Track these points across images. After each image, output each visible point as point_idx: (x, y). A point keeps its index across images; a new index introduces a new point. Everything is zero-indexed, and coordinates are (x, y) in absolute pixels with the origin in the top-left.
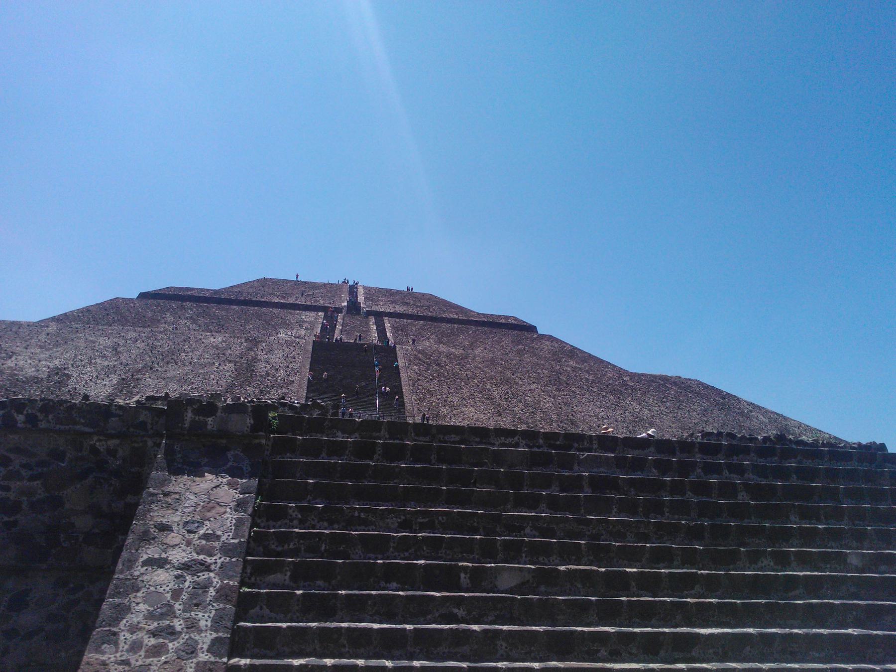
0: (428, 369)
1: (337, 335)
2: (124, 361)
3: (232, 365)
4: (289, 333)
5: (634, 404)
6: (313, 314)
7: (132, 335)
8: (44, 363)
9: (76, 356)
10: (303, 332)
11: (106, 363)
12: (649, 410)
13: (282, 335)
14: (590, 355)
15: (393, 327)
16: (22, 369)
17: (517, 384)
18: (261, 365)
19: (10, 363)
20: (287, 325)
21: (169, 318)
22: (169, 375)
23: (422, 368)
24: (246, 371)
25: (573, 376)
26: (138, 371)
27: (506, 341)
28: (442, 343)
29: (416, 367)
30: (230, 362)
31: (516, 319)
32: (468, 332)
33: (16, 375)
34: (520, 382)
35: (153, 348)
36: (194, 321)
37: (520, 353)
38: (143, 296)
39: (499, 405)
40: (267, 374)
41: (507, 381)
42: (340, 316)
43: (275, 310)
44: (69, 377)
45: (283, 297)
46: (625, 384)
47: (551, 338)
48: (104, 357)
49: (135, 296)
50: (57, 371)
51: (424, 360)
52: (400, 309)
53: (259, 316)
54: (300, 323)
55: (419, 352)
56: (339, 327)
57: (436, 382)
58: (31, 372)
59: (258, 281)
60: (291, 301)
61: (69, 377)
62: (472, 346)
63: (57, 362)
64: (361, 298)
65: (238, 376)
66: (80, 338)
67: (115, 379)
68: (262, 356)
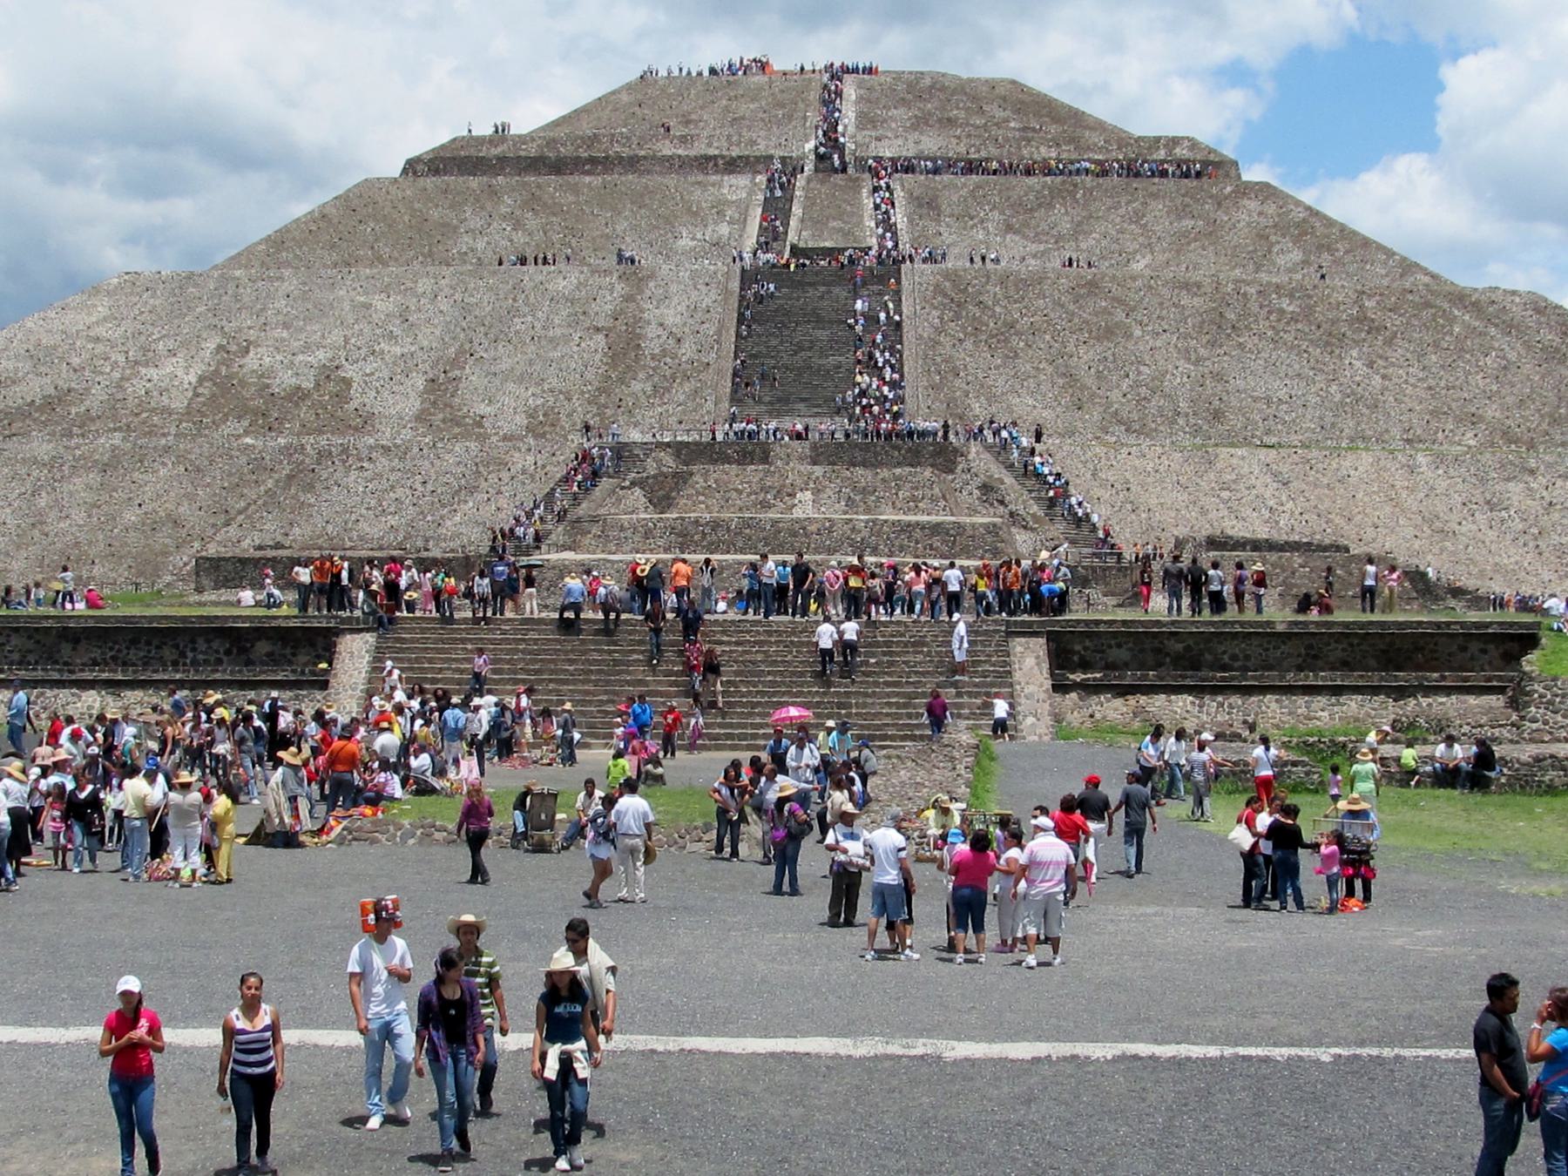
0: (957, 317)
1: (795, 234)
2: (425, 343)
3: (600, 337)
4: (699, 236)
5: (1358, 364)
6: (742, 181)
7: (424, 285)
8: (301, 357)
9: (346, 341)
10: (724, 229)
11: (398, 350)
12: (1384, 377)
13: (685, 243)
14: (1342, 228)
15: (911, 197)
16: (268, 373)
17: (1128, 336)
18: (652, 331)
19: (251, 361)
20: (696, 216)
21: (476, 223)
22: (504, 367)
23: (948, 315)
24: (625, 347)
25: (1255, 308)
26: (455, 362)
27: (1158, 207)
28: (1009, 228)
29: (935, 313)
30: (598, 330)
31: (1194, 144)
32: (1073, 194)
33: (268, 386)
34: (1138, 333)
35: (466, 309)
36: (518, 225)
37: (1182, 242)
38: (411, 167)
39: (1083, 387)
40: (664, 353)
41: (1109, 333)
42: (800, 181)
43: (671, 180)
44: (347, 383)
45: (683, 140)
46: (1362, 318)
47: (1265, 191)
48: (391, 336)
49: (396, 172)
50: (328, 373)
51: (956, 297)
52: (931, 143)
53: (639, 200)
54: (720, 208)
55: (947, 275)
56: (797, 210)
57: (969, 345)
58: (285, 380)
59: (629, 87)
60: (699, 148)
61: (347, 383)
62: (1078, 231)
63: (321, 354)
64: (848, 115)
65: (614, 366)
66: (340, 300)
67: (420, 383)
68: (651, 312)
